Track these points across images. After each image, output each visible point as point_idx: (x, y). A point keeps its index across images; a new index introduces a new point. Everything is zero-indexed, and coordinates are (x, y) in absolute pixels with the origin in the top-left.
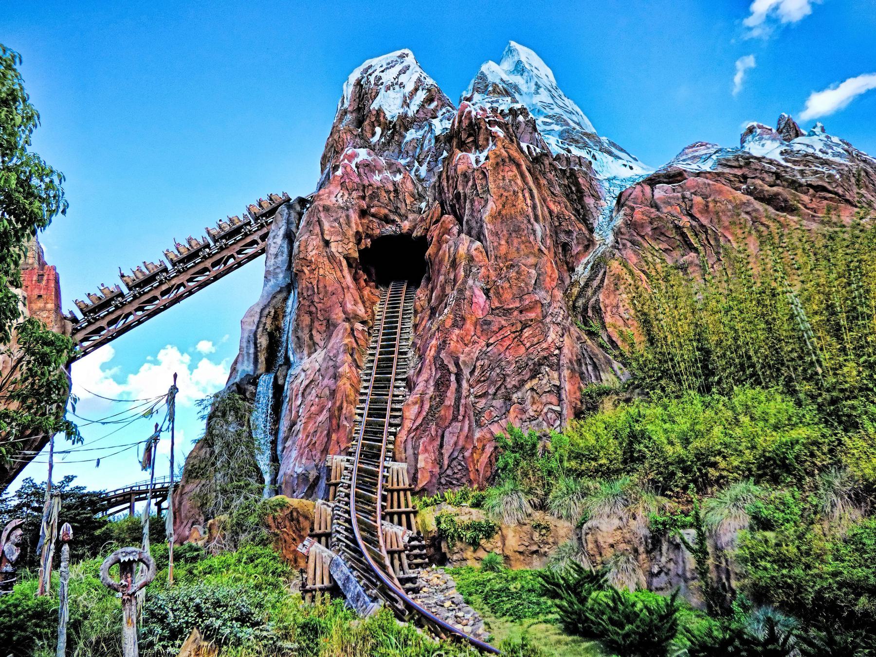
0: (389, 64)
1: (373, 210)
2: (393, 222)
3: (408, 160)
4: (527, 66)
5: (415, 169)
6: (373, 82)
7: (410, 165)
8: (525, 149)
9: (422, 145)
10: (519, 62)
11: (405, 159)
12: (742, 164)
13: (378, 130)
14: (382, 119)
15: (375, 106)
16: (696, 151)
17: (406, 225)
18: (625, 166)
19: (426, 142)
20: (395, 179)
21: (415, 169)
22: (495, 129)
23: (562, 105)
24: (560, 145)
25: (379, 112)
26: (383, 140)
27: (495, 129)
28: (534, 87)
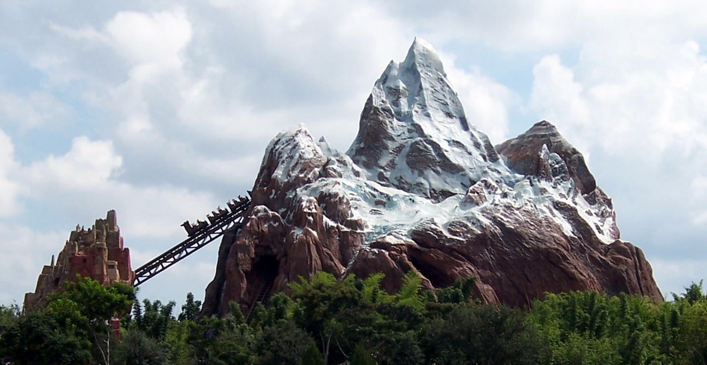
0: (287, 142)
1: (262, 244)
2: (271, 249)
3: (285, 209)
4: (419, 69)
5: (288, 215)
6: (277, 156)
7: (286, 212)
8: (324, 225)
9: (292, 202)
10: (414, 64)
11: (284, 208)
12: (423, 234)
13: (274, 191)
14: (276, 184)
15: (274, 175)
16: (539, 129)
17: (275, 250)
18: (410, 199)
19: (294, 201)
20: (275, 225)
21: (288, 215)
22: (311, 218)
23: (441, 97)
24: (373, 192)
25: (275, 180)
26: (275, 197)
27: (311, 218)
28: (418, 89)
